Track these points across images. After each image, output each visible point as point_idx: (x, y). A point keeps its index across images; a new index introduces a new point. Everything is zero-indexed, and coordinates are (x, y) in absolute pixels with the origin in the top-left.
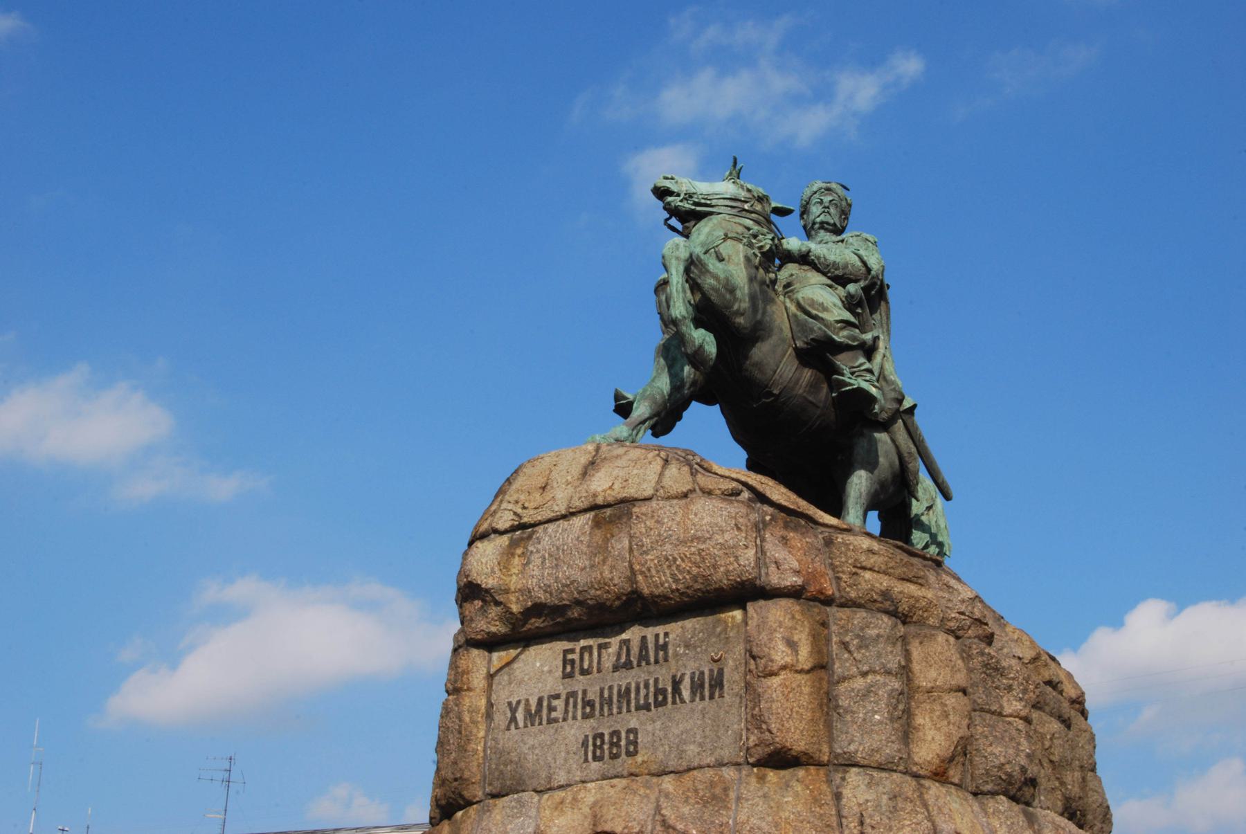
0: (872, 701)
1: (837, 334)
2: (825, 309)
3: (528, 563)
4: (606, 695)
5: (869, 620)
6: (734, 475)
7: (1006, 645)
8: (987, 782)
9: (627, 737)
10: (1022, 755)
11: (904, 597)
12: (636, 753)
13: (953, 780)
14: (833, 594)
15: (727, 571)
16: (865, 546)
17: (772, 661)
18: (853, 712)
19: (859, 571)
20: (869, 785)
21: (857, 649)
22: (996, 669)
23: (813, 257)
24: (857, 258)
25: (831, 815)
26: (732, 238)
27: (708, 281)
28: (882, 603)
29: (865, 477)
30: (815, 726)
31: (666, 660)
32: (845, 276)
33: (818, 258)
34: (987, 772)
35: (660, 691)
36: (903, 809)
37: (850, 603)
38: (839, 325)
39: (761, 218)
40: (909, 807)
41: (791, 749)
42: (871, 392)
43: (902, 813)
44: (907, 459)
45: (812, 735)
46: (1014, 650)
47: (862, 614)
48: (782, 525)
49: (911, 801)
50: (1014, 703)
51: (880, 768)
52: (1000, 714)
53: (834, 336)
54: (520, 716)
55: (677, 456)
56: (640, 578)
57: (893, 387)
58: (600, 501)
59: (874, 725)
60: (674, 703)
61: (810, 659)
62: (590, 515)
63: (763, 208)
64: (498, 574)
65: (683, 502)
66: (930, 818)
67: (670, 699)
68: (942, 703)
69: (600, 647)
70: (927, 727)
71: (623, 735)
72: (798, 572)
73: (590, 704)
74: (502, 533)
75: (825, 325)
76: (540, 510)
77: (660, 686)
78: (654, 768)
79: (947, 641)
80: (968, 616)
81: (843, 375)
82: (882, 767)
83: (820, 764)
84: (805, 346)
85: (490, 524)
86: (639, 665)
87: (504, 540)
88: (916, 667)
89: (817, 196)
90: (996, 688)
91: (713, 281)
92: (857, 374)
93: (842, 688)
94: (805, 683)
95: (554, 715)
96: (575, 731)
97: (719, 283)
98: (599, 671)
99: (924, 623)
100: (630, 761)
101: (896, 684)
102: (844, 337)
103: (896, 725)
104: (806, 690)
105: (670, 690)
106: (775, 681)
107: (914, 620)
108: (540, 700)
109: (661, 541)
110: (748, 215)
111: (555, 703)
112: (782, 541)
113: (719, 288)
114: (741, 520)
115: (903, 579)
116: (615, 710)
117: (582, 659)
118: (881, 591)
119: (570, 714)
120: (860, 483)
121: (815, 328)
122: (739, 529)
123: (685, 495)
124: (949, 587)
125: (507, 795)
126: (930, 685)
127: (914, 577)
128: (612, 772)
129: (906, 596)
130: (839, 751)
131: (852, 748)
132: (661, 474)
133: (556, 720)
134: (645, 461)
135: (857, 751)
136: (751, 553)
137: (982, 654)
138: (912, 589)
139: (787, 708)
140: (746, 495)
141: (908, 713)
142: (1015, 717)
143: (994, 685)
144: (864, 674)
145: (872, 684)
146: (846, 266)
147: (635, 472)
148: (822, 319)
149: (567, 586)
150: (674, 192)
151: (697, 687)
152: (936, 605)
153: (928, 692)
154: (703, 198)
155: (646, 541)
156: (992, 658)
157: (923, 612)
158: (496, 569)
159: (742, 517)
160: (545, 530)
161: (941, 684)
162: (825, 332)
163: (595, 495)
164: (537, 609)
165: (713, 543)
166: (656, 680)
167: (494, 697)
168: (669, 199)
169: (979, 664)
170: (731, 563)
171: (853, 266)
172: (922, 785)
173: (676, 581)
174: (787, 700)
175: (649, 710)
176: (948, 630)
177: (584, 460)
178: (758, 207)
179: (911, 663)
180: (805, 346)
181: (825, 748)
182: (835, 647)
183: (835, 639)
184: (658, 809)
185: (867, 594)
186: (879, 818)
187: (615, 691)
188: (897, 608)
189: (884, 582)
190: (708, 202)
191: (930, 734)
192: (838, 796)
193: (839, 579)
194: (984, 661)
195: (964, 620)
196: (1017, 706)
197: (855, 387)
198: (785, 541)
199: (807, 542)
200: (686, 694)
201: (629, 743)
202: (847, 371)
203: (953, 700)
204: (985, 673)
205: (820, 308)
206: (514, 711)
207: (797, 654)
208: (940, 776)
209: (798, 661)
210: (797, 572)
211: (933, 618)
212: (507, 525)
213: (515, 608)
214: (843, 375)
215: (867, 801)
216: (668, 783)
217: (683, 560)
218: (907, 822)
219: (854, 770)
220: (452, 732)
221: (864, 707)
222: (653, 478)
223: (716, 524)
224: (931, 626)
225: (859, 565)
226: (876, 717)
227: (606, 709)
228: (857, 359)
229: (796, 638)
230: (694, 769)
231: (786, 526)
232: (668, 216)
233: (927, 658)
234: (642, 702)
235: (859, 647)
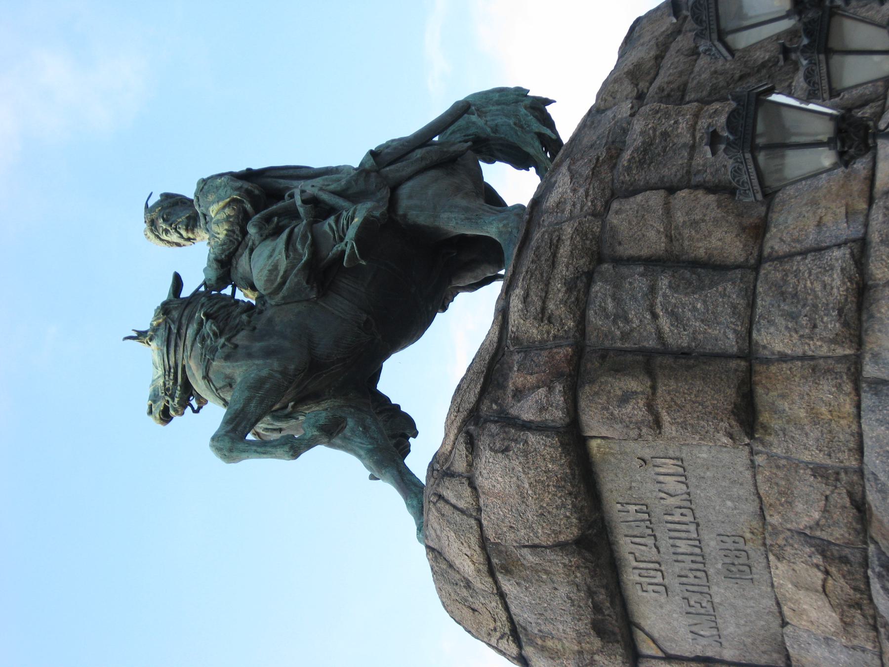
0: (683, 311)
1: (301, 255)
2: (275, 268)
5: (598, 307)
7: (618, 124)
11: (572, 264)
13: (763, 214)
14: (570, 345)
15: (553, 460)
18: (694, 332)
19: (547, 315)
20: (771, 323)
21: (628, 323)
22: (645, 151)
23: (223, 256)
25: (802, 366)
27: (253, 409)
28: (579, 291)
29: (449, 214)
30: (710, 375)
32: (240, 223)
33: (223, 251)
36: (795, 287)
37: (580, 327)
38: (291, 253)
39: (186, 313)
40: (792, 280)
41: (735, 404)
42: (359, 224)
43: (799, 288)
44: (428, 162)
45: (719, 380)
46: (625, 115)
48: (501, 391)
49: (786, 275)
50: (679, 131)
53: (303, 261)
55: (435, 486)
56: (562, 538)
57: (353, 183)
58: (484, 568)
59: (708, 310)
61: (641, 378)
62: (500, 577)
63: (176, 308)
68: (682, 226)
70: (708, 245)
72: (550, 389)
75: (293, 268)
76: (496, 616)
79: (617, 213)
80: (589, 184)
81: (343, 252)
82: (751, 302)
83: (750, 371)
84: (315, 289)
88: (645, 252)
90: (664, 151)
92: (341, 234)
94: (665, 385)
97: (254, 397)
99: (598, 238)
101: (664, 282)
102: (303, 249)
103: (707, 282)
104: (673, 384)
107: (595, 249)
110: (183, 331)
112: (518, 397)
113: (259, 397)
115: (553, 263)
118: (566, 292)
120: (456, 220)
121: (296, 280)
125: (787, 650)
126: (663, 239)
127: (550, 248)
129: (570, 262)
131: (731, 336)
135: (735, 331)
137: (628, 169)
138: (564, 251)
139: (692, 408)
141: (695, 264)
142: (695, 130)
143: (662, 154)
144: (655, 316)
145: (664, 311)
148: (285, 272)
152: (579, 223)
153: (671, 241)
154: (169, 376)
156: (633, 158)
157: (587, 239)
159: (494, 443)
161: (662, 227)
162: (299, 270)
169: (640, 174)
173: (563, 506)
174: (684, 406)
176: (605, 209)
179: (641, 256)
180: (315, 289)
181: (733, 364)
182: (627, 345)
183: (619, 344)
185: (570, 308)
186: (805, 318)
188: (584, 273)
189: (558, 285)
190: (172, 370)
191: (714, 242)
192: (783, 358)
194: (637, 167)
195: (594, 189)
198: (518, 393)
199: (518, 370)
202: (339, 247)
203: (679, 214)
204: (649, 165)
205: (275, 273)
207: (636, 393)
209: (643, 393)
210: (551, 389)
211: (593, 228)
213: (597, 643)
214: (343, 252)
216: (774, 519)
217: (542, 500)
218: (809, 284)
219: (755, 335)
224: (601, 229)
225: (540, 315)
226: (699, 306)
228: (325, 232)
229: (619, 393)
231: (503, 387)
232: (189, 408)
233: (636, 239)
235: (627, 321)
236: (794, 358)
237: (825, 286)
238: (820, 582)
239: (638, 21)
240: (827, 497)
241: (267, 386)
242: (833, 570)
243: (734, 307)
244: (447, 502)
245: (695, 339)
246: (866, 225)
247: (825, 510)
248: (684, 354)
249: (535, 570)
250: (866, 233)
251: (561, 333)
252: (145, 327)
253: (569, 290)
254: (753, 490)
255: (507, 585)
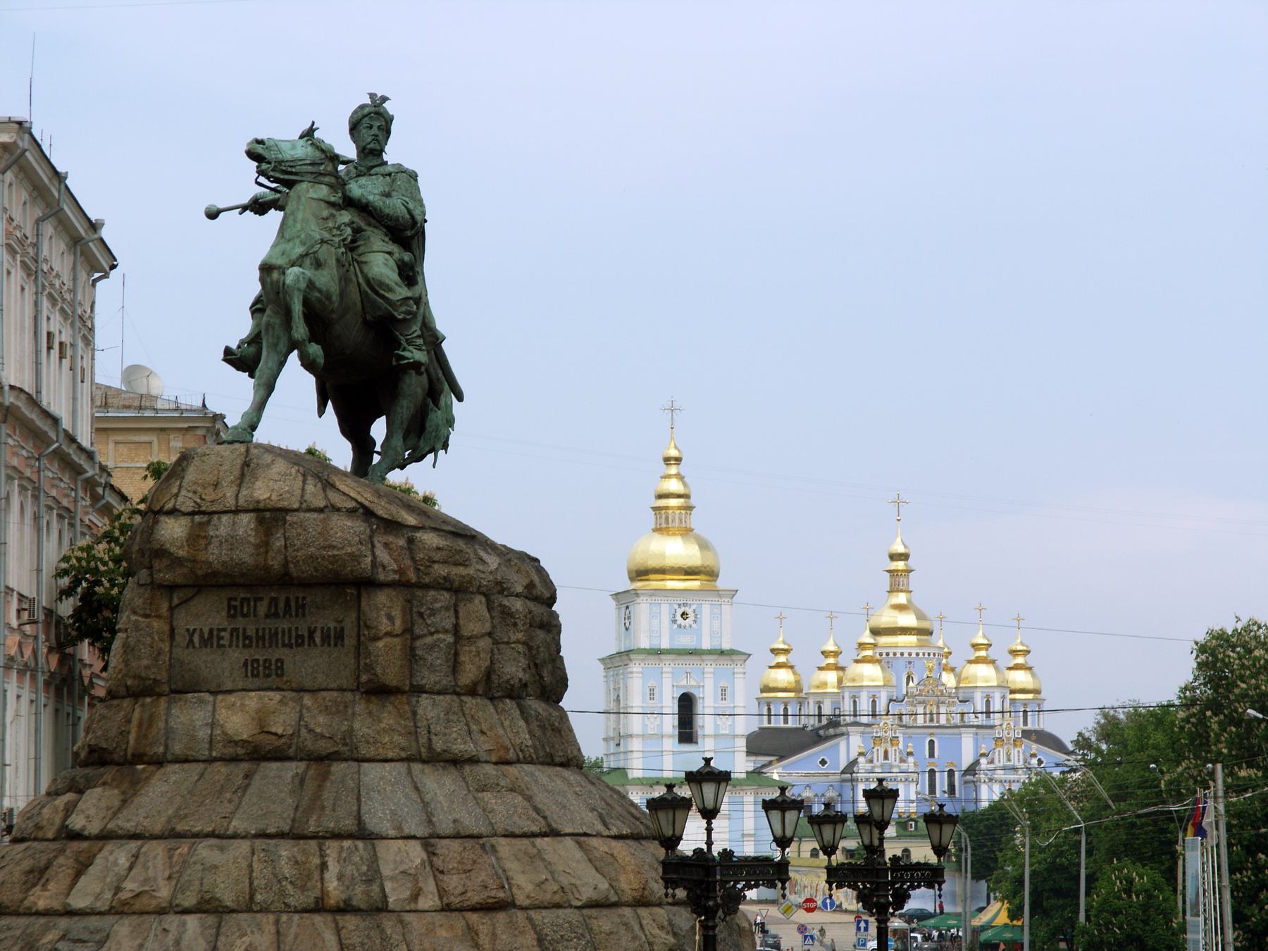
2: (390, 290)
3: (210, 543)
4: (260, 634)
6: (352, 494)
8: (498, 691)
9: (276, 664)
10: (520, 670)
12: (282, 675)
15: (352, 571)
16: (434, 546)
17: (380, 630)
24: (406, 211)
26: (326, 242)
31: (304, 615)
33: (375, 209)
34: (499, 685)
35: (298, 636)
40: (454, 718)
47: (432, 593)
51: (439, 693)
52: (508, 643)
54: (196, 639)
58: (261, 505)
60: (309, 645)
64: (186, 548)
65: (322, 516)
66: (467, 725)
67: (306, 643)
69: (256, 600)
71: (273, 662)
73: (249, 638)
74: (184, 514)
77: (300, 633)
78: (294, 685)
79: (481, 602)
83: (402, 692)
85: (175, 505)
86: (284, 616)
87: (188, 519)
88: (461, 622)
89: (366, 119)
91: (317, 294)
93: (418, 643)
95: (222, 642)
96: (237, 655)
98: (255, 616)
100: (278, 680)
102: (402, 313)
104: (398, 647)
105: (306, 635)
106: (380, 644)
108: (211, 631)
109: (306, 544)
110: (322, 179)
111: (223, 634)
114: (362, 537)
116: (267, 645)
117: (242, 606)
119: (234, 643)
122: (361, 543)
123: (321, 510)
124: (482, 560)
126: (470, 634)
128: (266, 685)
130: (415, 683)
131: (424, 682)
132: (303, 489)
133: (223, 646)
134: (291, 478)
136: (369, 559)
137: (500, 605)
138: (462, 571)
140: (361, 511)
141: (456, 654)
144: (432, 634)
146: (397, 219)
147: (287, 488)
149: (240, 565)
150: (266, 159)
151: (326, 638)
155: (298, 543)
158: (185, 544)
160: (219, 519)
163: (258, 502)
164: (215, 574)
165: (344, 552)
166: (297, 628)
167: (175, 623)
168: (264, 166)
170: (355, 566)
171: (403, 218)
172: (461, 700)
173: (316, 570)
175: (291, 647)
177: (239, 462)
178: (330, 168)
181: (407, 682)
184: (301, 717)
187: (267, 631)
190: (294, 170)
191: (469, 667)
192: (414, 713)
193: (419, 569)
196: (520, 636)
197: (411, 361)
200: (318, 640)
201: (277, 668)
206: (192, 634)
207: (393, 624)
208: (472, 692)
212: (190, 509)
215: (432, 718)
216: (307, 700)
217: (323, 559)
218: (455, 729)
220: (144, 645)
221: (431, 655)
222: (298, 492)
223: (347, 539)
227: (260, 643)
229: (393, 614)
230: (323, 690)
234: (286, 642)
235: (429, 616)
236: (415, 723)
237: (456, 739)
238: (273, 730)
239: (537, 560)
240: (331, 738)
241: (327, 303)
242: (283, 740)
243: (439, 682)
244: (304, 482)
245: (421, 659)
246: (486, 762)
247: (322, 736)
248: (412, 649)
249: (265, 545)
250: (482, 762)
251: (421, 574)
252: (317, 135)
253: (445, 578)
254: (323, 687)
255: (245, 519)
